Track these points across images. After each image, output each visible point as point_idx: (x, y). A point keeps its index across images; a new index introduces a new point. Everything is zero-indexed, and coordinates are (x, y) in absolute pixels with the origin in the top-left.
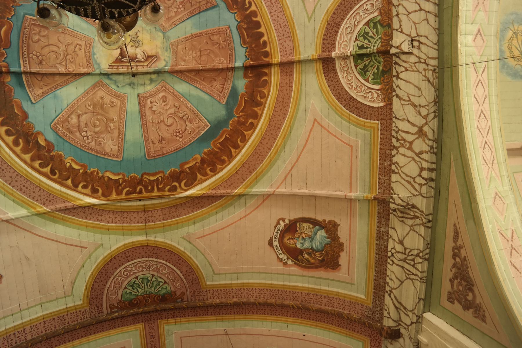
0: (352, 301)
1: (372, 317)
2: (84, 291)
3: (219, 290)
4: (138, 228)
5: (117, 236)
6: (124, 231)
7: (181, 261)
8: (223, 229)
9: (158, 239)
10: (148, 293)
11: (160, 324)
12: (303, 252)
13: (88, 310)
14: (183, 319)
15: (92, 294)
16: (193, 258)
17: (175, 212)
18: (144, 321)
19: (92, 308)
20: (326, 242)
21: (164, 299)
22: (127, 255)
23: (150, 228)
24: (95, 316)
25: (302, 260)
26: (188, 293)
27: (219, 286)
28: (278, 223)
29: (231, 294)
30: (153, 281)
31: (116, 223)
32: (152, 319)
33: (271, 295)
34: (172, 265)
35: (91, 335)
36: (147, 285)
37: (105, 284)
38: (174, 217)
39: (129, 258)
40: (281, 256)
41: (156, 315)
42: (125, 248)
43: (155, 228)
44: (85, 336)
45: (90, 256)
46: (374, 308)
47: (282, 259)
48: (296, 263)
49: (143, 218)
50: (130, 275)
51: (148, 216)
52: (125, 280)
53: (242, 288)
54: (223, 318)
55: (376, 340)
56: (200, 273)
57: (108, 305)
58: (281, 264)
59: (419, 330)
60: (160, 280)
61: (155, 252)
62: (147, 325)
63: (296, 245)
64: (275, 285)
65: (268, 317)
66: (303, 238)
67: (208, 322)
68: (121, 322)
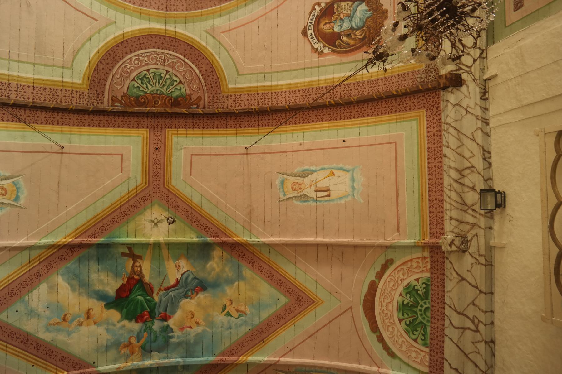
0: (400, 73)
1: (426, 80)
2: (85, 69)
3: (242, 96)
4: (158, 14)
5: (133, 18)
6: (141, 15)
7: (202, 57)
8: (252, 22)
9: (178, 30)
10: (159, 92)
11: (168, 134)
12: (342, 35)
13: (87, 95)
14: (197, 131)
15: (94, 75)
16: (215, 55)
17: (201, 3)
18: (150, 127)
19: (91, 93)
20: (367, 16)
21: (176, 102)
22: (141, 42)
23: (170, 17)
24: (93, 105)
25: (340, 46)
26: (206, 98)
27: (243, 90)
28: (314, 9)
29: (256, 101)
30: (167, 79)
31: (134, 4)
32: (159, 127)
33: (304, 97)
34: (191, 61)
35: (84, 126)
36: (159, 83)
37: (111, 68)
38: (199, 8)
39: (142, 45)
40: (316, 46)
41: (165, 122)
42: (140, 33)
43: (177, 17)
44: (78, 126)
45: (99, 31)
46: (427, 68)
47: (317, 49)
48: (333, 51)
49: (165, 5)
50: (141, 66)
51: (170, 4)
52: (135, 70)
53: (270, 92)
54: (245, 131)
55: (433, 106)
56: (222, 74)
57: (110, 96)
58: (316, 55)
59: (484, 69)
60: (175, 78)
61: (173, 44)
62: (152, 133)
63: (333, 30)
64: (309, 82)
65: (299, 126)
66: (341, 19)
67: (227, 137)
68: (122, 121)
